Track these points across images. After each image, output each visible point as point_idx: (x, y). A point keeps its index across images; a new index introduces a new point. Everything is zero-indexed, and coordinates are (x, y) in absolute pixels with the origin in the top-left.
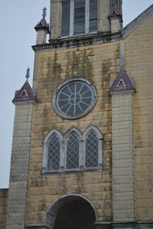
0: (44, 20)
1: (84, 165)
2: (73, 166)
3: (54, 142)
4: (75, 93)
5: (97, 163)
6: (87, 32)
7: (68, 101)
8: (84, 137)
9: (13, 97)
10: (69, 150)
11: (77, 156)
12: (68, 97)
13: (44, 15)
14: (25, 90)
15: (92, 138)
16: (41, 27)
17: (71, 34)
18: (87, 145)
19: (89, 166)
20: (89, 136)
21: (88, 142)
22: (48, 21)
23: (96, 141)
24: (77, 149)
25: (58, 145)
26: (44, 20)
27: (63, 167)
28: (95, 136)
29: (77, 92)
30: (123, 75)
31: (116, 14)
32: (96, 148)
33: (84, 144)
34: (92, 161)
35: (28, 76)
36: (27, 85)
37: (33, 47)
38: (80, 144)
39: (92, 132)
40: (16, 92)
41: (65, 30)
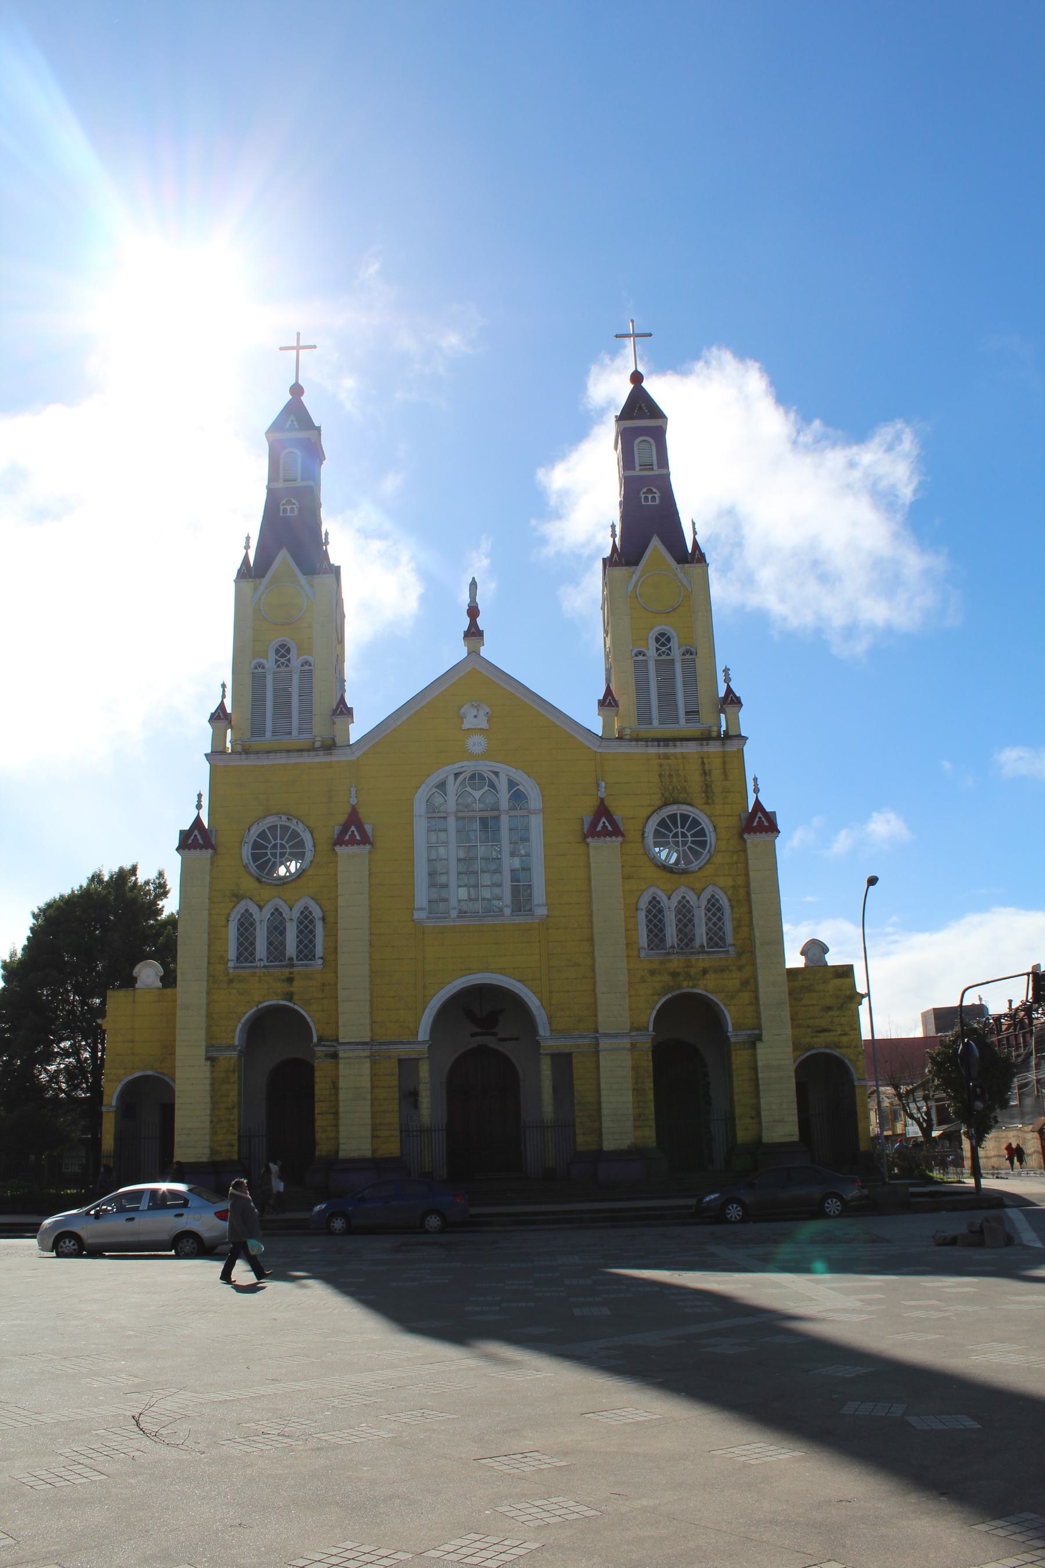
0: (222, 706)
1: (295, 958)
4: (279, 841)
5: (314, 956)
6: (295, 732)
7: (266, 854)
8: (296, 914)
9: (177, 844)
10: (270, 933)
11: (283, 944)
12: (266, 848)
13: (224, 696)
15: (306, 917)
16: (219, 717)
17: (268, 734)
18: (298, 927)
19: (301, 960)
20: (302, 913)
21: (301, 922)
22: (229, 710)
23: (312, 922)
24: (282, 933)
25: (252, 924)
26: (222, 706)
27: (261, 960)
29: (282, 839)
30: (354, 819)
31: (343, 711)
32: (312, 932)
33: (295, 924)
34: (306, 950)
35: (199, 806)
36: (198, 821)
37: (206, 755)
38: (288, 925)
40: (181, 831)
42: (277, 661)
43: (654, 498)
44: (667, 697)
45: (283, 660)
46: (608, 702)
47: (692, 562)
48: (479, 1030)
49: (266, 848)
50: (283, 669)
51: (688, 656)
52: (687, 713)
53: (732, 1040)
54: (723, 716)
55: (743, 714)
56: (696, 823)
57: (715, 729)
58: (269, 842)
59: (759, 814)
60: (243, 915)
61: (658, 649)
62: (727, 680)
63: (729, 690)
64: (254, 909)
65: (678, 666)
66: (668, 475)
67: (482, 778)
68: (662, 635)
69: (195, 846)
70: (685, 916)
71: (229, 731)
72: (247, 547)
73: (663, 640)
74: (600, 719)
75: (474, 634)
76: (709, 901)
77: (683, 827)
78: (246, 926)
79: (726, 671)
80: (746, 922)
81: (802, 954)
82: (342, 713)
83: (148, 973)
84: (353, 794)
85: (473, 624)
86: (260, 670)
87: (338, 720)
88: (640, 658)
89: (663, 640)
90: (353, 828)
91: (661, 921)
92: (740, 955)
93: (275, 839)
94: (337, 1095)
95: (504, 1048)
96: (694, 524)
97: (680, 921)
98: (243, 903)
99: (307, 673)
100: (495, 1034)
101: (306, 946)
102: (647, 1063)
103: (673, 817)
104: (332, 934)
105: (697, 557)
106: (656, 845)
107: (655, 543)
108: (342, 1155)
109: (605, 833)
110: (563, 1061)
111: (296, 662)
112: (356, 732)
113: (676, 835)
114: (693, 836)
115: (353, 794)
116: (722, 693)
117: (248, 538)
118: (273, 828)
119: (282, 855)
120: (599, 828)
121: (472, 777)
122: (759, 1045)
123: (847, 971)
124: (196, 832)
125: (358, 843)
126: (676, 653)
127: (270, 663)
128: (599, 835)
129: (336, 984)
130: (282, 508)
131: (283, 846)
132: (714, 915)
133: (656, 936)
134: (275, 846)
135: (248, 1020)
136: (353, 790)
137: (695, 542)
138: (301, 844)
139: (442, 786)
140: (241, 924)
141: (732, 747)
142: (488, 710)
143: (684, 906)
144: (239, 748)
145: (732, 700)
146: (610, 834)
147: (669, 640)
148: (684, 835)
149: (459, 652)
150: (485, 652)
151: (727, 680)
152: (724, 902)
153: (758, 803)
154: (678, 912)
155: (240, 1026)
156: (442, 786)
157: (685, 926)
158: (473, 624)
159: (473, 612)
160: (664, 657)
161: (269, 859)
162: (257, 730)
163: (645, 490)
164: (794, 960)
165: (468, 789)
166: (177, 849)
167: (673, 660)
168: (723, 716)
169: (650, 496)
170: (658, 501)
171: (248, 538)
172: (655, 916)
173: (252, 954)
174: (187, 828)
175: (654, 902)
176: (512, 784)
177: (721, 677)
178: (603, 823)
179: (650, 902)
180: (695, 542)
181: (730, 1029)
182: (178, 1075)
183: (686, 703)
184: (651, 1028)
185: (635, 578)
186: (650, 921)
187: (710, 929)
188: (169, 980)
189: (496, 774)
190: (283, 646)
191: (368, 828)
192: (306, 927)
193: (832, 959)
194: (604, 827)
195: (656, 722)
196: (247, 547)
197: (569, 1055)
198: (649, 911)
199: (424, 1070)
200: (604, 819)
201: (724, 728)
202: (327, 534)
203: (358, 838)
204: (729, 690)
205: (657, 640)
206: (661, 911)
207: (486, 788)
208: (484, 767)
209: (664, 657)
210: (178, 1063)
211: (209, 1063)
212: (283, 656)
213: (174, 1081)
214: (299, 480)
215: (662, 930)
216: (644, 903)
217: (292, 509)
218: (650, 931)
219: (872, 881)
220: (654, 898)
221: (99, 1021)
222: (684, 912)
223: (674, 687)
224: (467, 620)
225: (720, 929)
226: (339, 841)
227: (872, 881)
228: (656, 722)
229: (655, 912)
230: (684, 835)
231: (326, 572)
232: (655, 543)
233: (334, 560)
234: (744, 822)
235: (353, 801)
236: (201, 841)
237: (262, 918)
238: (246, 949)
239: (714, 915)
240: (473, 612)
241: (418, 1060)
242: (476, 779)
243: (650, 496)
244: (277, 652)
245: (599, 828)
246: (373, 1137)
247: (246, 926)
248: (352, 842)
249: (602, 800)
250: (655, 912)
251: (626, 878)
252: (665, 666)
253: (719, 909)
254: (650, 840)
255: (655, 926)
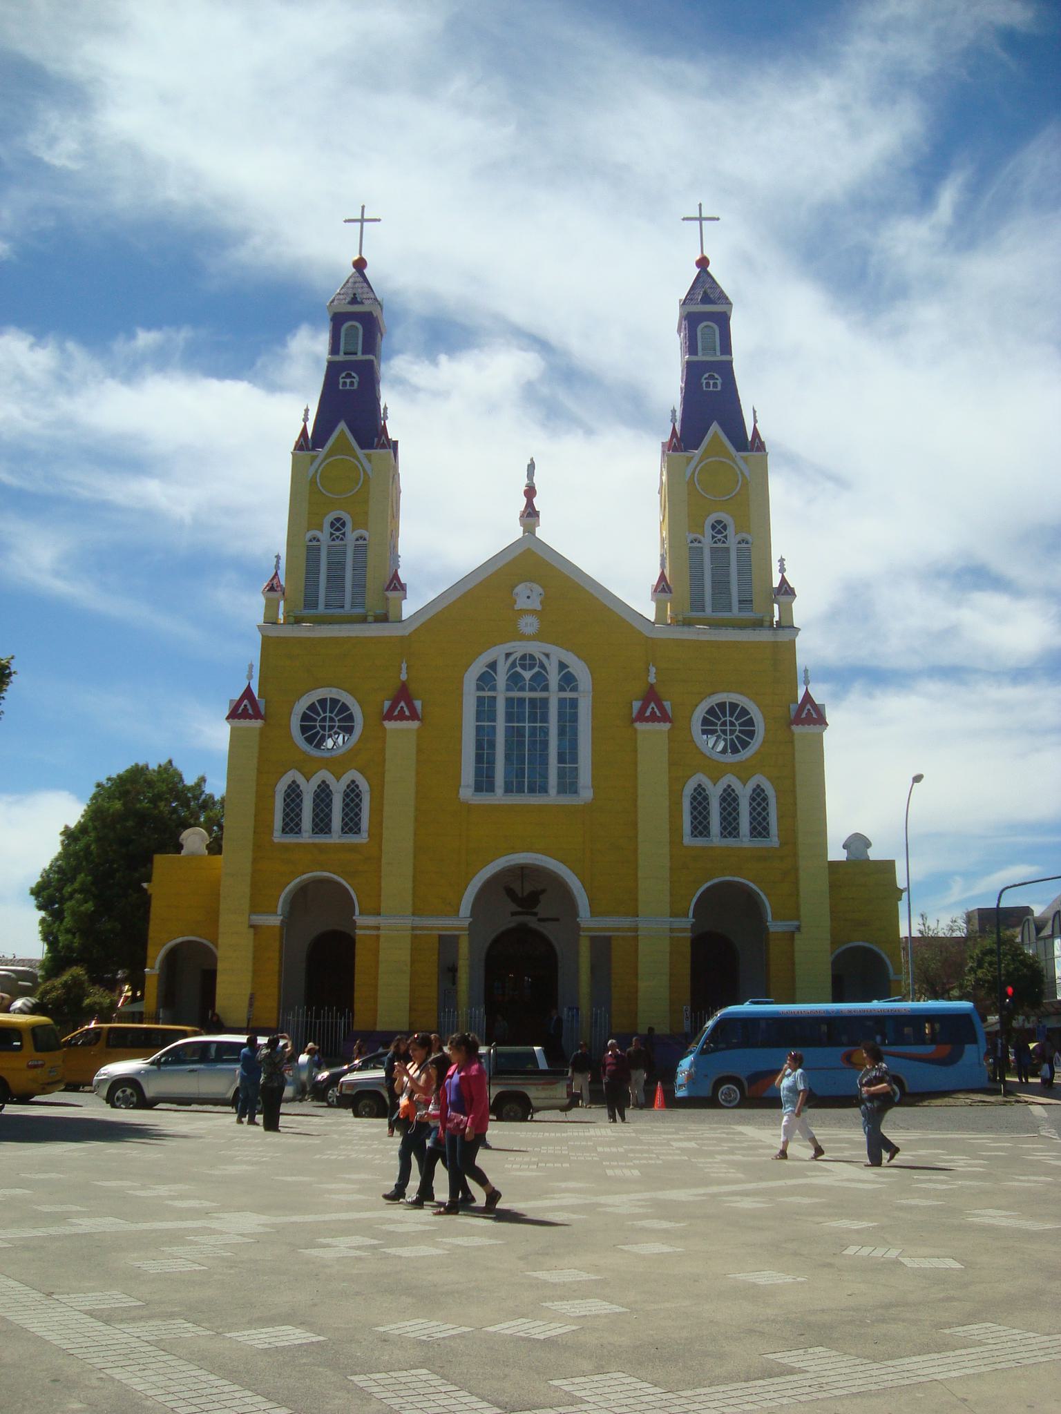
2: (322, 831)
3: (293, 791)
6: (347, 606)
10: (316, 805)
12: (315, 720)
14: (246, 702)
15: (353, 791)
17: (321, 607)
21: (346, 795)
23: (358, 795)
24: (329, 805)
28: (357, 786)
34: (351, 825)
35: (250, 677)
36: (248, 693)
39: (353, 782)
40: (231, 701)
41: (310, 602)
42: (332, 534)
43: (715, 385)
44: (721, 585)
45: (338, 533)
46: (662, 587)
47: (752, 450)
48: (520, 909)
49: (315, 720)
50: (337, 542)
51: (744, 545)
52: (740, 602)
53: (771, 930)
54: (776, 606)
55: (796, 606)
56: (744, 712)
57: (768, 619)
58: (319, 715)
59: (809, 707)
60: (289, 786)
61: (713, 537)
62: (782, 570)
63: (784, 581)
64: (301, 780)
65: (733, 555)
66: (731, 362)
67: (532, 657)
68: (719, 522)
69: (245, 715)
70: (729, 804)
71: (282, 603)
72: (306, 420)
73: (719, 528)
74: (653, 605)
75: (530, 514)
76: (754, 790)
77: (731, 715)
78: (293, 794)
79: (782, 561)
80: (789, 814)
81: (844, 847)
82: (395, 589)
83: (194, 839)
84: (404, 670)
85: (530, 504)
86: (315, 543)
87: (390, 594)
88: (696, 544)
89: (719, 528)
90: (402, 704)
91: (705, 808)
92: (783, 844)
93: (325, 712)
94: (377, 967)
95: (547, 929)
96: (755, 412)
97: (724, 809)
98: (290, 773)
99: (361, 549)
100: (535, 914)
101: (351, 820)
102: (687, 949)
103: (722, 706)
104: (377, 811)
105: (757, 445)
106: (704, 732)
107: (715, 428)
108: (378, 1028)
109: (653, 718)
110: (602, 945)
111: (351, 535)
112: (409, 608)
113: (724, 724)
114: (740, 725)
115: (404, 670)
116: (776, 584)
117: (307, 411)
118: (322, 702)
119: (331, 728)
120: (648, 714)
121: (523, 657)
122: (797, 936)
123: (889, 866)
124: (246, 702)
125: (407, 718)
126: (732, 542)
127: (324, 536)
128: (647, 720)
129: (380, 859)
130: (341, 381)
131: (332, 719)
132: (759, 804)
133: (700, 823)
134: (324, 719)
135: (290, 891)
136: (404, 666)
137: (755, 430)
138: (350, 718)
139: (493, 666)
140: (287, 795)
141: (783, 636)
142: (541, 590)
143: (729, 795)
144: (292, 620)
145: (786, 591)
146: (658, 720)
147: (725, 528)
148: (732, 724)
149: (517, 532)
150: (540, 533)
151: (782, 570)
152: (770, 792)
153: (807, 695)
154: (723, 799)
155: (283, 895)
156: (493, 666)
157: (730, 814)
158: (530, 504)
159: (530, 492)
160: (720, 545)
161: (318, 732)
162: (310, 602)
163: (706, 375)
164: (836, 853)
165: (518, 669)
166: (228, 718)
167: (727, 550)
168: (776, 606)
169: (711, 382)
170: (719, 388)
171: (307, 411)
172: (700, 803)
173: (298, 825)
174: (237, 698)
175: (700, 790)
176: (562, 666)
177: (775, 567)
178: (652, 705)
179: (695, 790)
180: (755, 430)
181: (770, 918)
182: (220, 941)
183: (740, 591)
184: (691, 914)
185: (693, 463)
186: (694, 808)
187: (754, 819)
188: (215, 847)
189: (547, 656)
190: (338, 520)
191: (418, 704)
192: (352, 800)
193: (874, 854)
194: (653, 713)
195: (709, 609)
196: (306, 420)
197: (609, 939)
198: (694, 798)
199: (464, 948)
200: (653, 705)
201: (776, 618)
202: (386, 409)
203: (407, 713)
204: (784, 581)
205: (713, 527)
206: (706, 798)
207: (536, 669)
208: (535, 648)
209: (720, 545)
210: (221, 930)
211: (252, 930)
212: (338, 529)
213: (217, 946)
214: (360, 353)
215: (706, 818)
216: (689, 789)
217: (352, 384)
218: (695, 818)
219: (918, 779)
220: (700, 785)
221: (145, 885)
222: (729, 799)
223: (728, 575)
224: (524, 500)
225: (764, 819)
226: (389, 716)
227: (918, 779)
228: (709, 609)
229: (700, 800)
230: (732, 724)
231: (383, 446)
232: (715, 428)
233: (392, 435)
234: (793, 713)
235: (404, 677)
236: (250, 711)
237: (308, 790)
238: (292, 820)
239: (759, 804)
240: (530, 492)
241: (457, 937)
242: (528, 661)
243: (711, 382)
244: (332, 525)
245: (648, 714)
246: (411, 1010)
247: (293, 794)
248: (402, 717)
249: (652, 686)
250: (700, 800)
251: (672, 764)
252: (720, 555)
253: (765, 799)
254: (696, 726)
255: (700, 813)
